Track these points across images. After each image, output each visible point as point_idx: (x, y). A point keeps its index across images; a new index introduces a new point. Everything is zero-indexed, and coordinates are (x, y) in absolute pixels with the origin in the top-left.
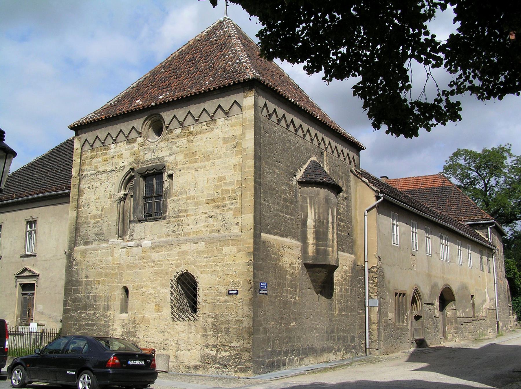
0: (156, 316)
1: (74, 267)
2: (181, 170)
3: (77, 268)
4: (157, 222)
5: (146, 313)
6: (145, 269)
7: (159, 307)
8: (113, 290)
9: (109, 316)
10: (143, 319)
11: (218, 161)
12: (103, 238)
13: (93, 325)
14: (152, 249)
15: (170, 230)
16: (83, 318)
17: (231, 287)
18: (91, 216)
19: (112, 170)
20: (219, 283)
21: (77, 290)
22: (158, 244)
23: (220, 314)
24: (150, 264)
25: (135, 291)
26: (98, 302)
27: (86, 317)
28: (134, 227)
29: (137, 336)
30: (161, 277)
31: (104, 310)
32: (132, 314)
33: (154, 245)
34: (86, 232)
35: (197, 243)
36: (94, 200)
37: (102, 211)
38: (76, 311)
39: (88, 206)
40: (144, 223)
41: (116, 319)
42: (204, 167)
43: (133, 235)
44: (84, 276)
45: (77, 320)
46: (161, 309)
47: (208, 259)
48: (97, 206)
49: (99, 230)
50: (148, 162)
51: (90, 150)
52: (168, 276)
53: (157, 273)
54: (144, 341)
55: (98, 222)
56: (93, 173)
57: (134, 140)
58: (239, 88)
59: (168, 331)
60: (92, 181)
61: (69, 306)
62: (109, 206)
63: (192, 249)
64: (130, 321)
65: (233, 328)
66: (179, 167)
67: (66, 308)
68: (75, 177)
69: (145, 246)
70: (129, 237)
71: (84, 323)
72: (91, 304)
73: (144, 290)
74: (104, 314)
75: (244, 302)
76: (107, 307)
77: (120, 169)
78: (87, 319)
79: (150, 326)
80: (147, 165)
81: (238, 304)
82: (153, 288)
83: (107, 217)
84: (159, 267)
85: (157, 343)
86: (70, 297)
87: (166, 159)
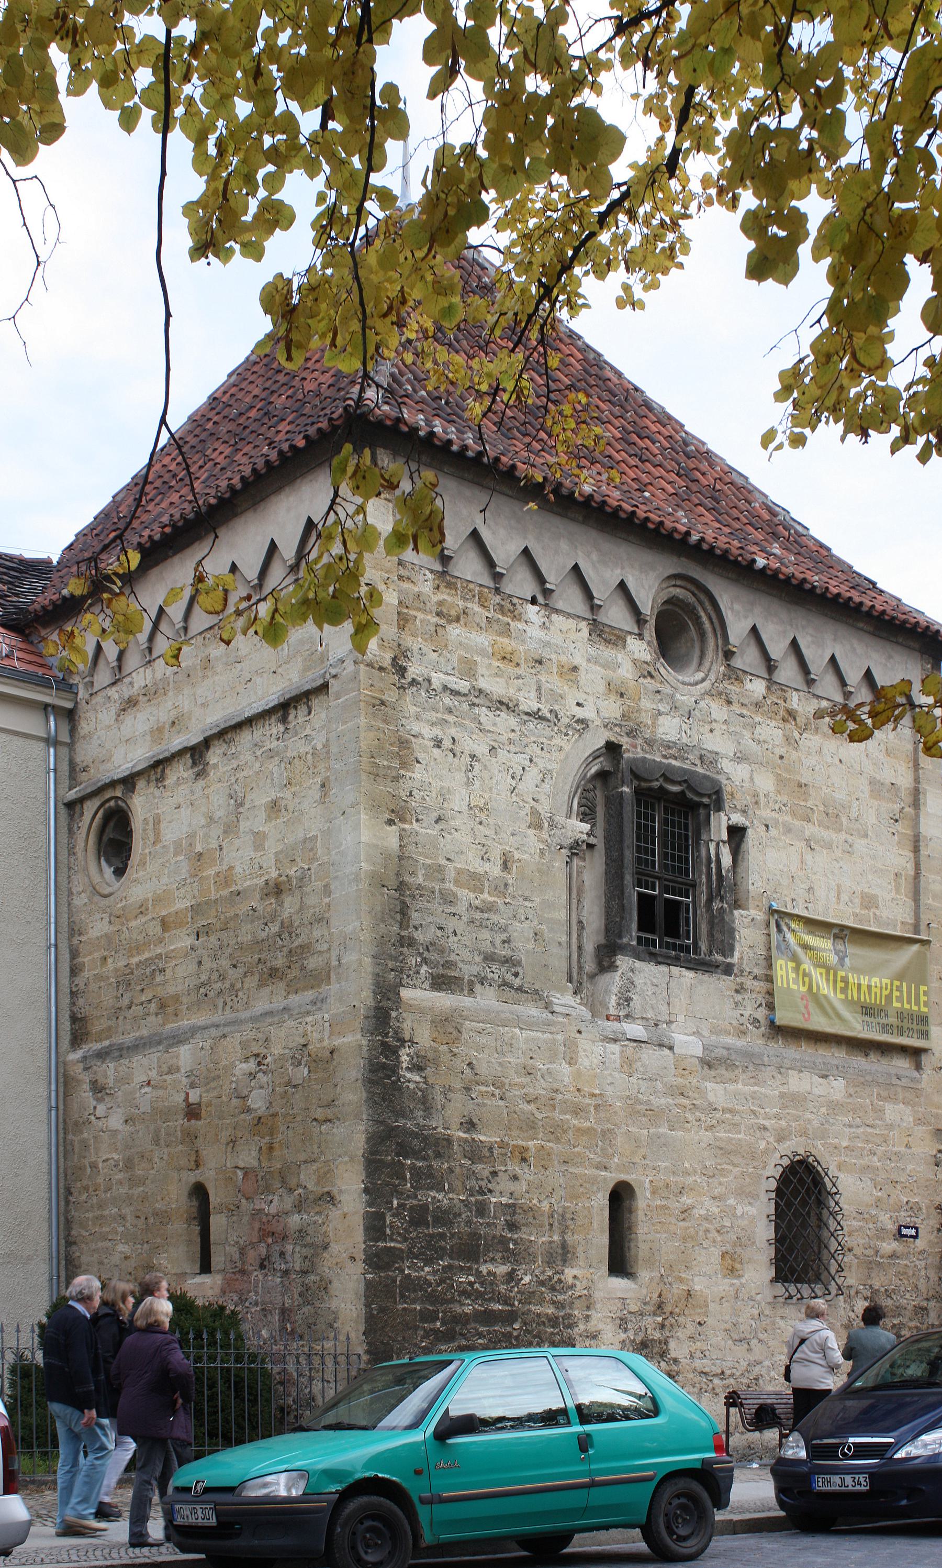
0: (727, 1288)
1: (409, 1075)
2: (767, 826)
3: (418, 1079)
4: (706, 977)
5: (696, 1279)
6: (689, 1131)
7: (734, 1260)
8: (581, 1190)
9: (572, 1287)
10: (687, 1300)
11: (860, 844)
12: (517, 982)
13: (511, 1317)
14: (706, 1067)
15: (747, 1014)
16: (464, 1293)
17: (905, 1219)
18: (459, 872)
19: (536, 715)
20: (878, 1203)
21: (431, 1176)
22: (725, 1053)
23: (883, 1289)
24: (702, 1117)
25: (659, 1202)
26: (524, 1229)
27: (476, 1286)
28: (632, 970)
29: (673, 1354)
30: (735, 1165)
31: (550, 1263)
32: (652, 1279)
33: (713, 1055)
34: (439, 933)
35: (825, 1077)
36: (465, 808)
37: (505, 866)
38: (428, 1262)
39: (436, 822)
40: (664, 968)
41: (598, 1295)
42: (829, 846)
43: (631, 999)
44: (455, 1121)
45: (433, 1298)
46: (738, 1266)
47: (852, 1130)
48: (484, 841)
49: (498, 942)
50: (669, 747)
51: (432, 571)
52: (755, 1164)
53: (724, 1151)
54: (694, 1370)
55: (489, 908)
56: (455, 687)
57: (618, 637)
58: (914, 649)
59: (761, 1336)
60: (451, 718)
61: (392, 1240)
62: (537, 857)
63: (816, 1091)
64: (645, 1304)
65: (910, 1328)
66: (765, 813)
67: (381, 1244)
68: (381, 669)
69: (684, 1051)
70: (618, 1004)
71: (468, 1310)
72: (494, 1237)
73: (686, 1200)
74: (550, 1278)
75: (929, 1261)
76: (560, 1251)
77: (569, 726)
78: (485, 1293)
79: (710, 1321)
80: (665, 757)
81: (917, 1263)
82: (714, 1198)
83: (525, 899)
84: (729, 1131)
85: (732, 1375)
86: (395, 1202)
87: (726, 765)
